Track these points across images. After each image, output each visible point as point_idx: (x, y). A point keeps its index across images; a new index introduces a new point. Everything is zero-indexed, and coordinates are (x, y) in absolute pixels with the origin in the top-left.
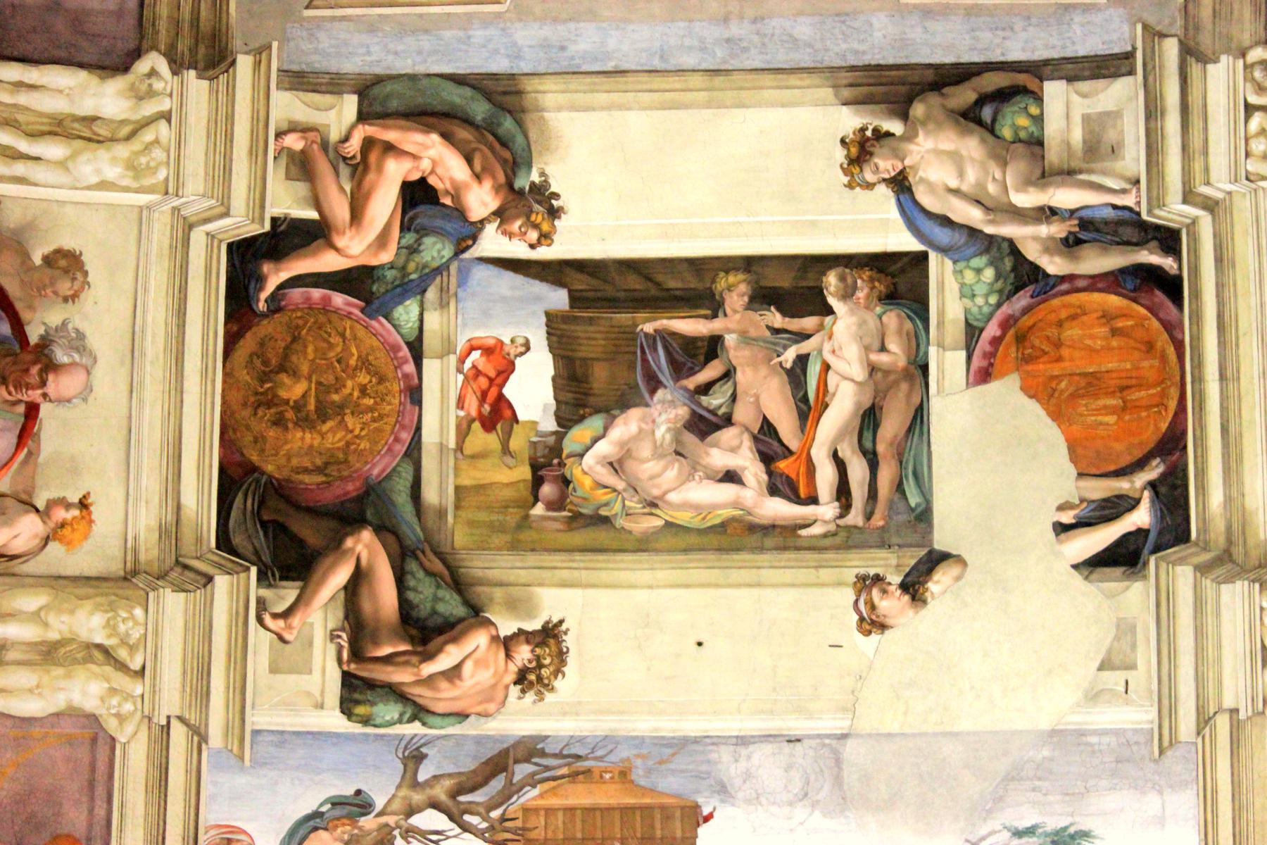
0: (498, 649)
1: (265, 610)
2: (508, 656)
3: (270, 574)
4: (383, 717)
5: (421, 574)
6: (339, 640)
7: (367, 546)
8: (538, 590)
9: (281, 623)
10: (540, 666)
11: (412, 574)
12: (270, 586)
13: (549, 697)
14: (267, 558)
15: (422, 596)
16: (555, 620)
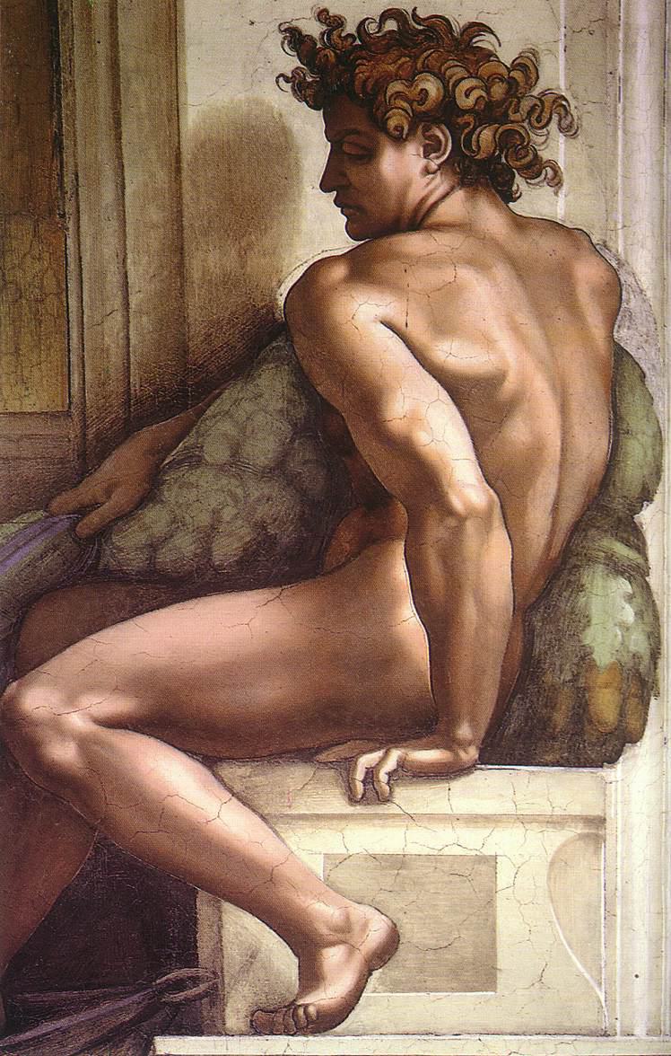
0: (397, 256)
1: (292, 1006)
2: (418, 219)
3: (181, 996)
4: (626, 628)
5: (155, 518)
6: (383, 777)
7: (71, 699)
8: (192, 118)
9: (332, 957)
10: (447, 111)
11: (153, 547)
12: (215, 996)
13: (554, 75)
14: (127, 1007)
15: (227, 513)
16: (290, 62)
